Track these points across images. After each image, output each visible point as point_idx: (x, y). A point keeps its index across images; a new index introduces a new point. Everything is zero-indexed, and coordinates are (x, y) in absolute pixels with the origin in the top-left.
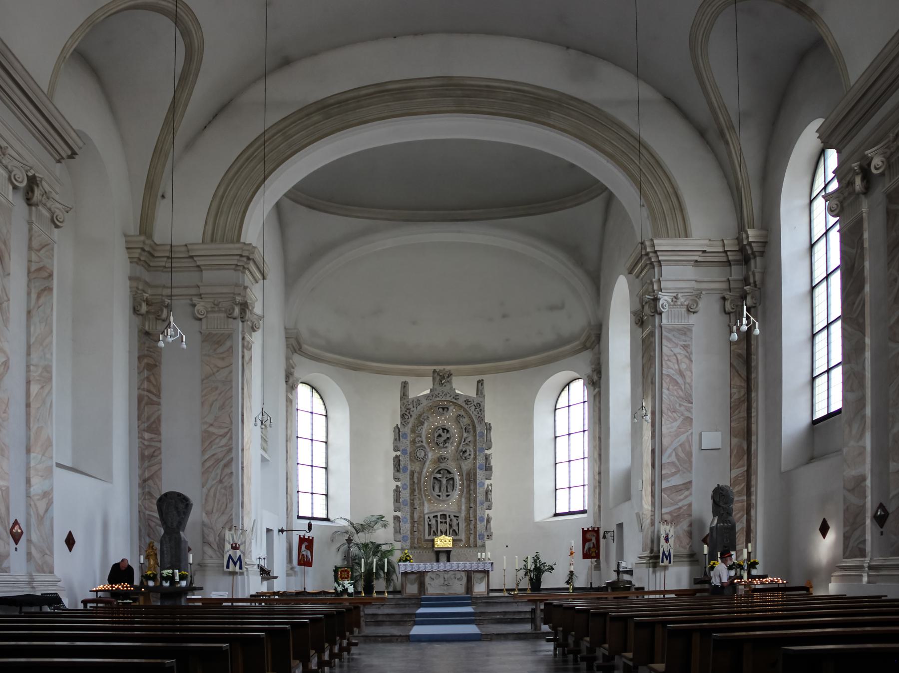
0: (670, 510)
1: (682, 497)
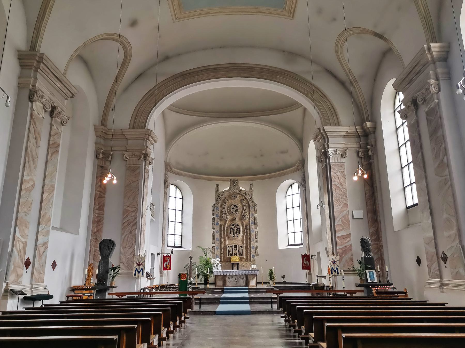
1: (346, 241)
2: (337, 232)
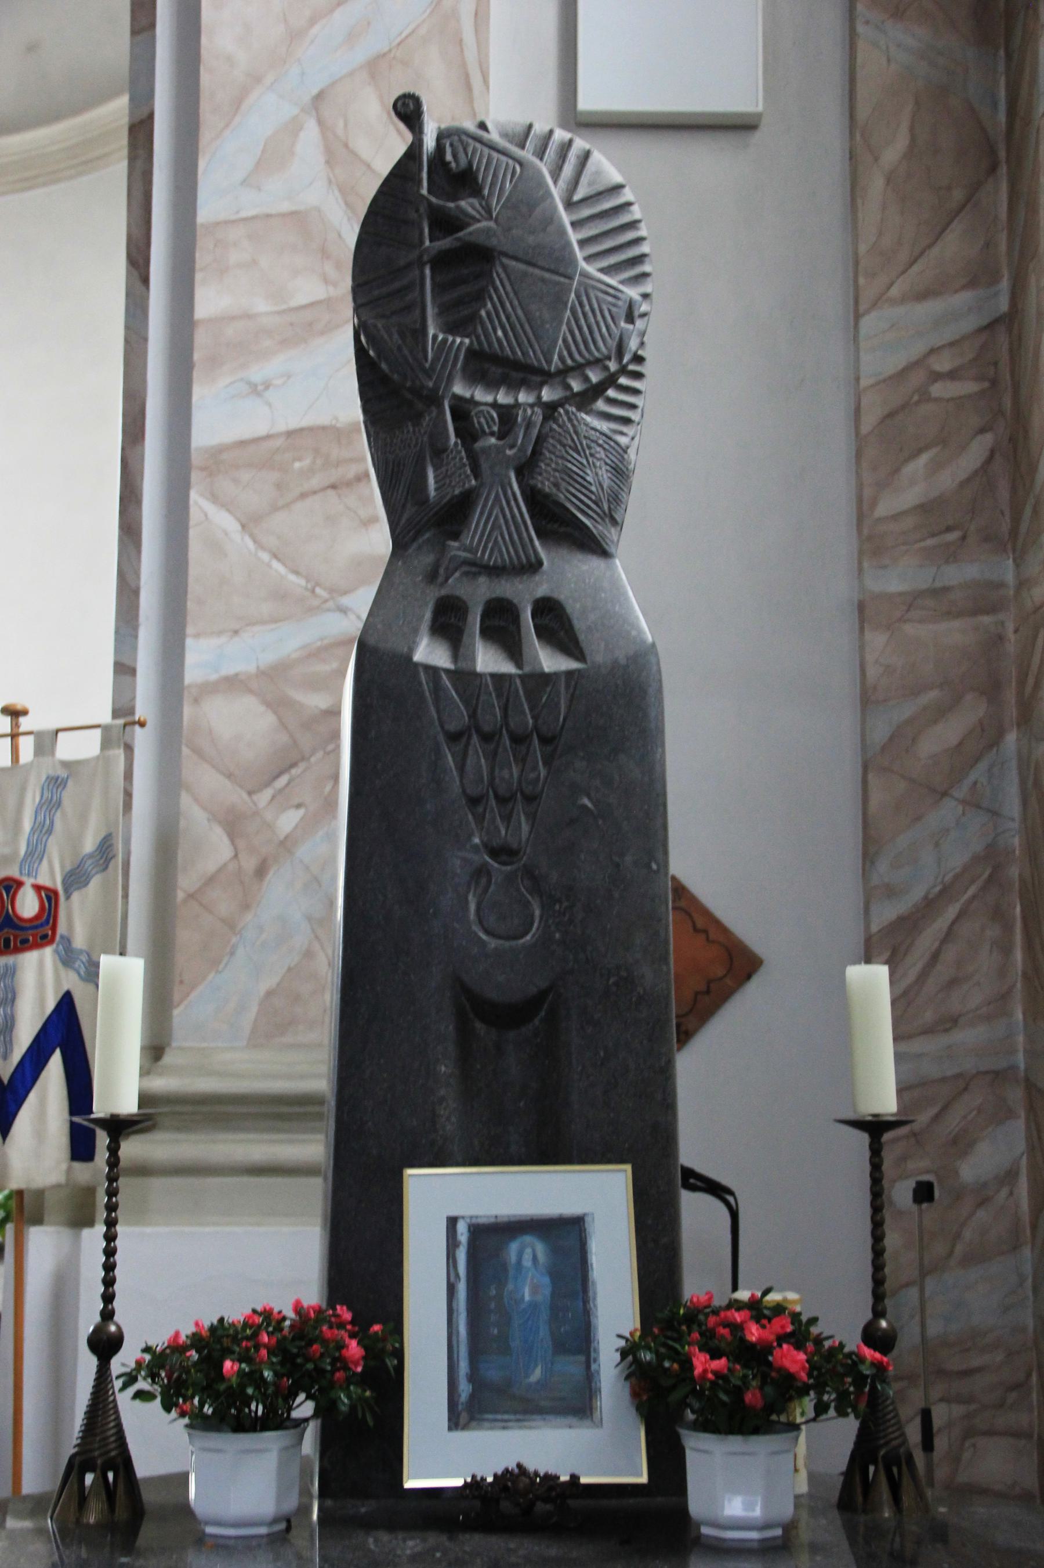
0: (268, 658)
2: (215, 362)
